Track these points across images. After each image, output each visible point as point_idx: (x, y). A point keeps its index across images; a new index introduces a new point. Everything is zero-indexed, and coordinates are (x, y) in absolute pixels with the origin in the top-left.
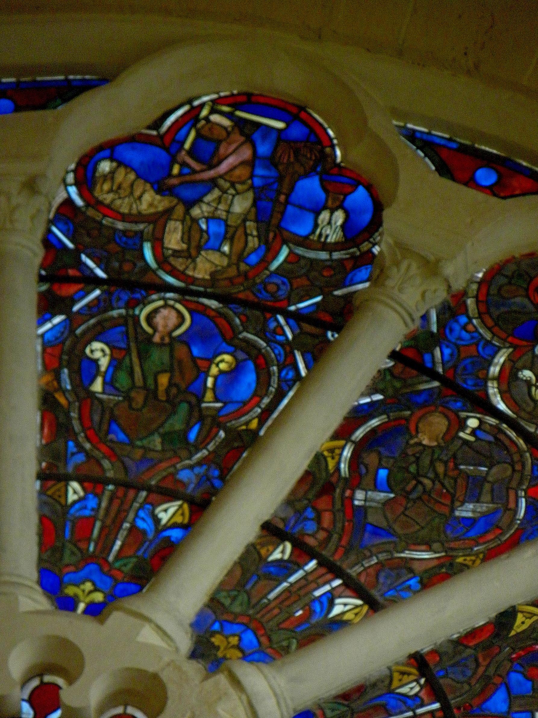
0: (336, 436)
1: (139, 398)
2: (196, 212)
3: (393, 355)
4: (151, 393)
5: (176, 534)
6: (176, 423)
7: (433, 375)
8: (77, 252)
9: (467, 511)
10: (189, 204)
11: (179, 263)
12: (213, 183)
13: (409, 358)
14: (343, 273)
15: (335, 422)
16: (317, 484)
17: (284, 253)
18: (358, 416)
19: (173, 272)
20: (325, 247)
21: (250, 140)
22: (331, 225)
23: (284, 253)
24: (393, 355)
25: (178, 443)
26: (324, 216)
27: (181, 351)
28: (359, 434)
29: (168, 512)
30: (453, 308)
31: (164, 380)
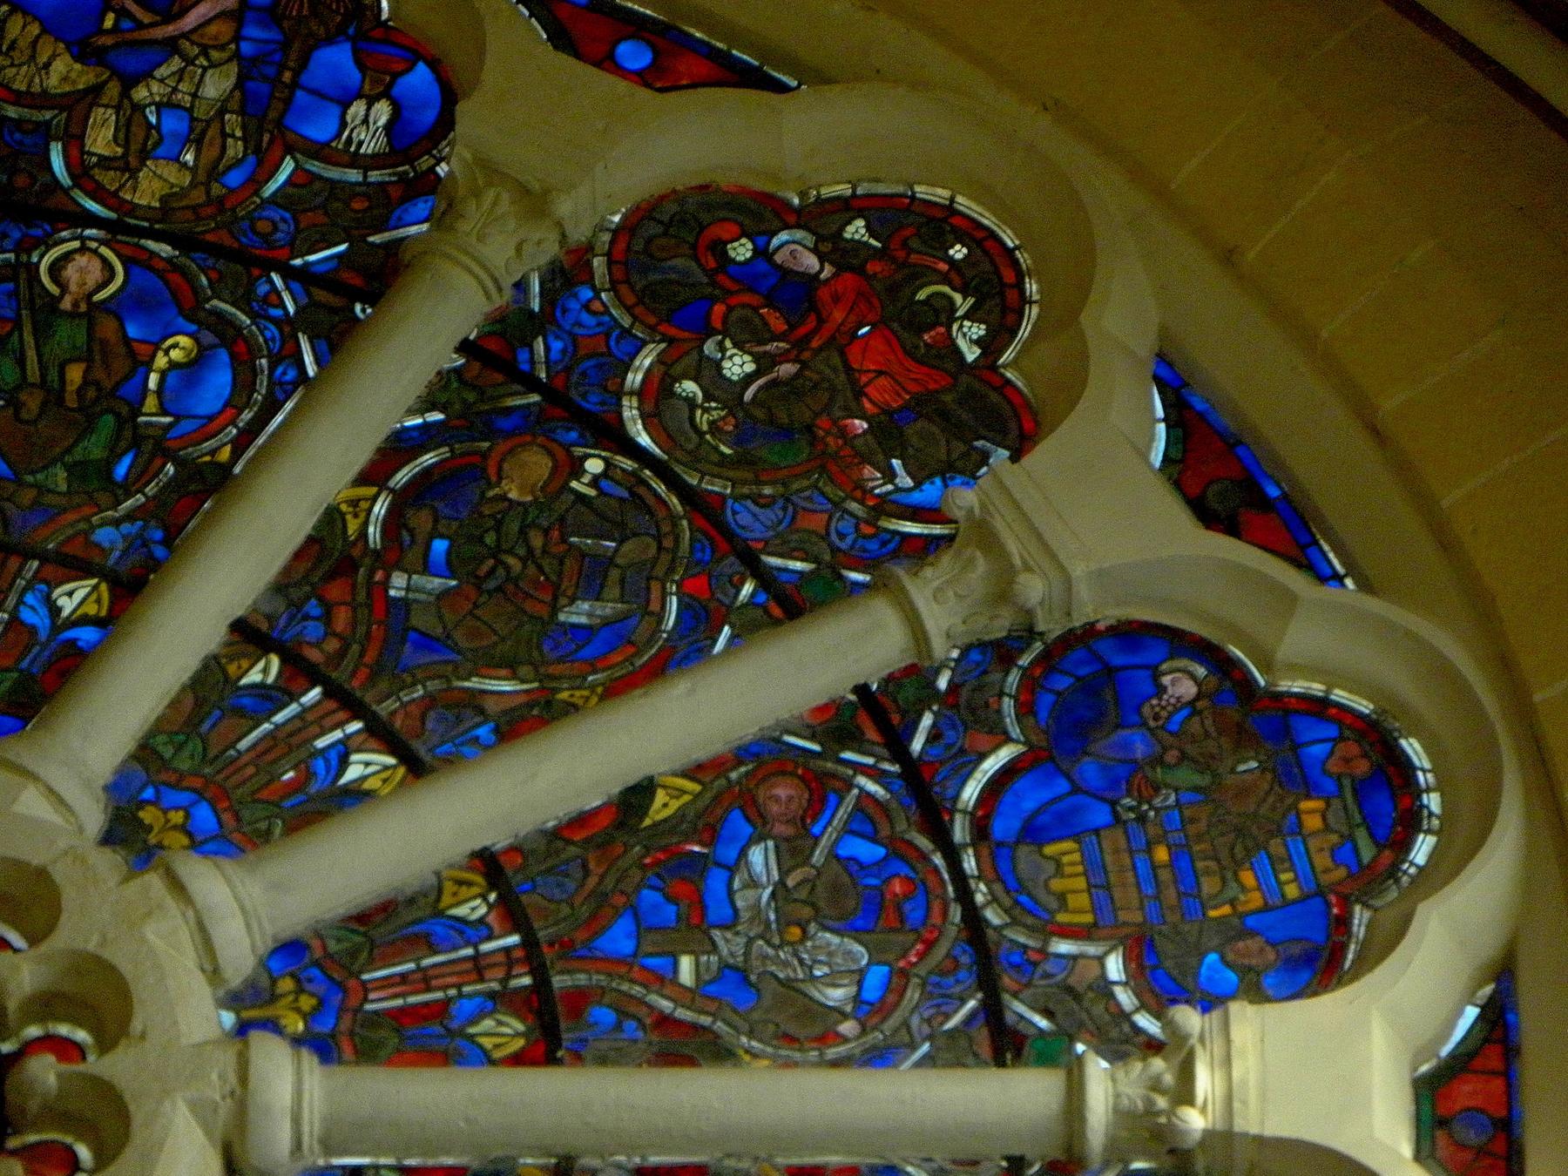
0: (363, 479)
1: (32, 403)
2: (140, 93)
3: (464, 347)
4: (54, 397)
5: (87, 635)
6: (94, 448)
7: (532, 384)
9: (578, 613)
10: (129, 81)
11: (108, 179)
12: (171, 46)
13: (491, 353)
14: (385, 206)
15: (361, 455)
16: (326, 557)
17: (288, 167)
18: (399, 447)
19: (98, 194)
20: (356, 161)
22: (369, 124)
23: (288, 167)
24: (464, 347)
25: (95, 481)
26: (357, 109)
27: (107, 327)
28: (402, 477)
29: (73, 597)
30: (567, 274)
31: (75, 374)
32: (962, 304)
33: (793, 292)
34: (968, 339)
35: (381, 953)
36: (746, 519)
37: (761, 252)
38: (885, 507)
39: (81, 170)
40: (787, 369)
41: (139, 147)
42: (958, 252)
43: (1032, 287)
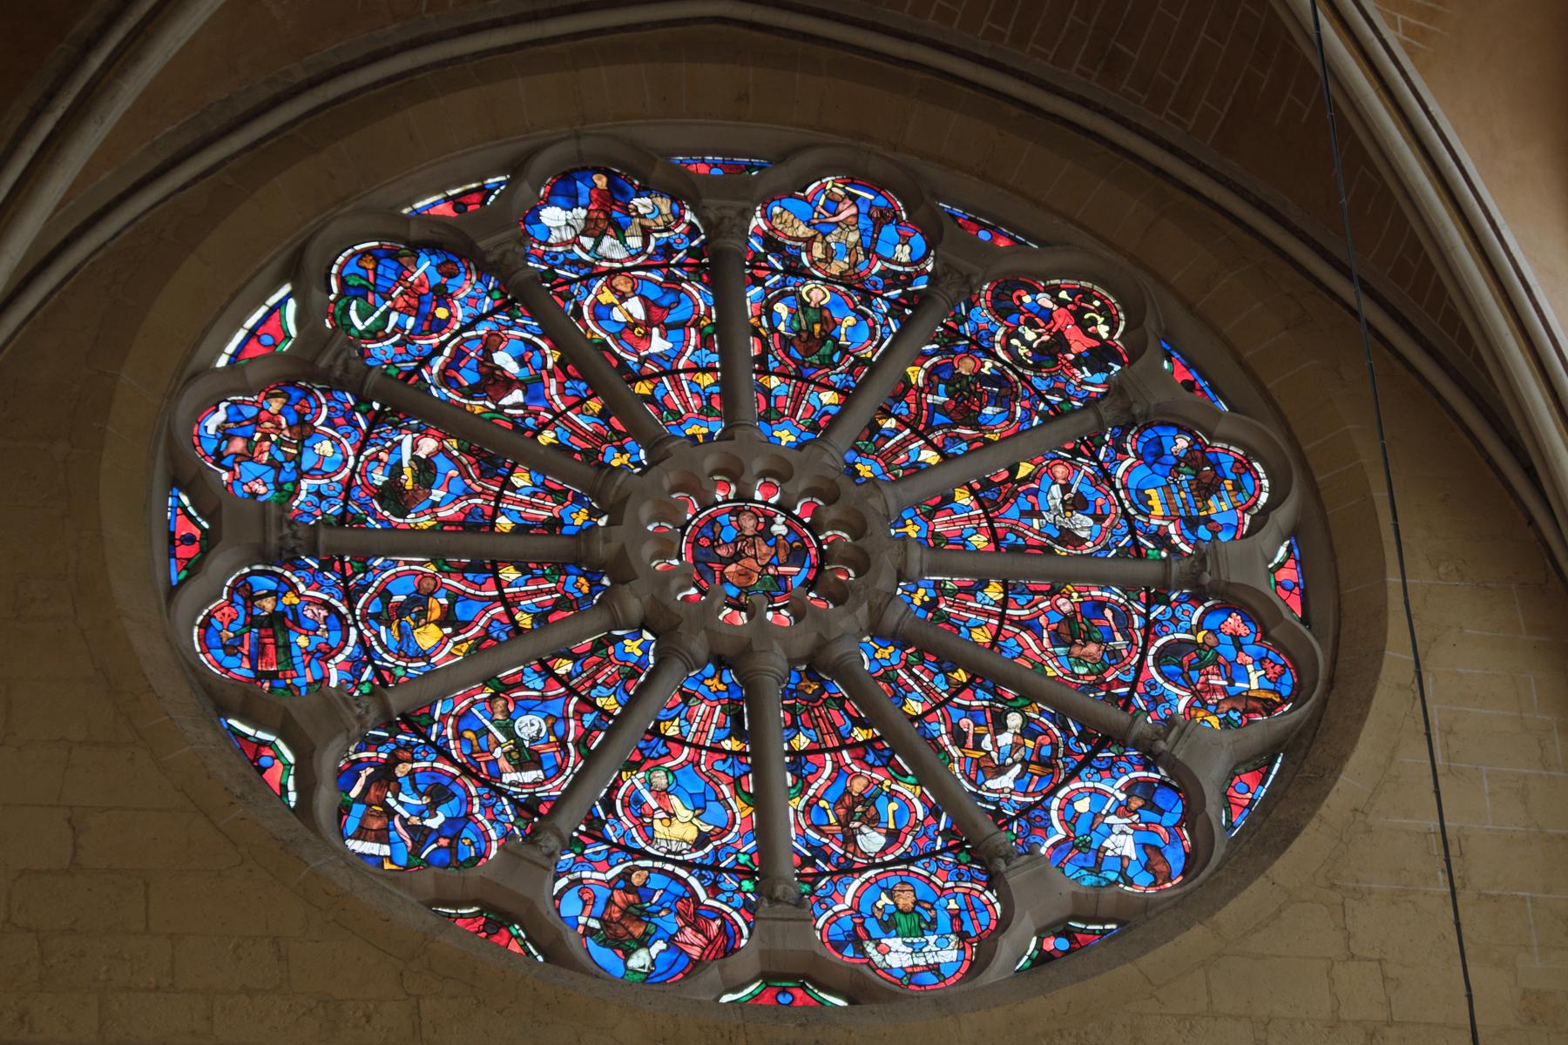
1: (804, 335)
2: (828, 239)
4: (811, 333)
6: (825, 350)
7: (965, 337)
8: (765, 255)
12: (837, 224)
14: (910, 278)
20: (900, 264)
21: (854, 203)
28: (927, 365)
29: (829, 397)
31: (817, 327)
32: (1100, 320)
33: (1048, 315)
34: (1103, 330)
36: (1037, 382)
37: (1034, 300)
38: (1083, 382)
39: (813, 263)
40: (1046, 338)
41: (829, 256)
42: (1097, 303)
43: (1122, 315)
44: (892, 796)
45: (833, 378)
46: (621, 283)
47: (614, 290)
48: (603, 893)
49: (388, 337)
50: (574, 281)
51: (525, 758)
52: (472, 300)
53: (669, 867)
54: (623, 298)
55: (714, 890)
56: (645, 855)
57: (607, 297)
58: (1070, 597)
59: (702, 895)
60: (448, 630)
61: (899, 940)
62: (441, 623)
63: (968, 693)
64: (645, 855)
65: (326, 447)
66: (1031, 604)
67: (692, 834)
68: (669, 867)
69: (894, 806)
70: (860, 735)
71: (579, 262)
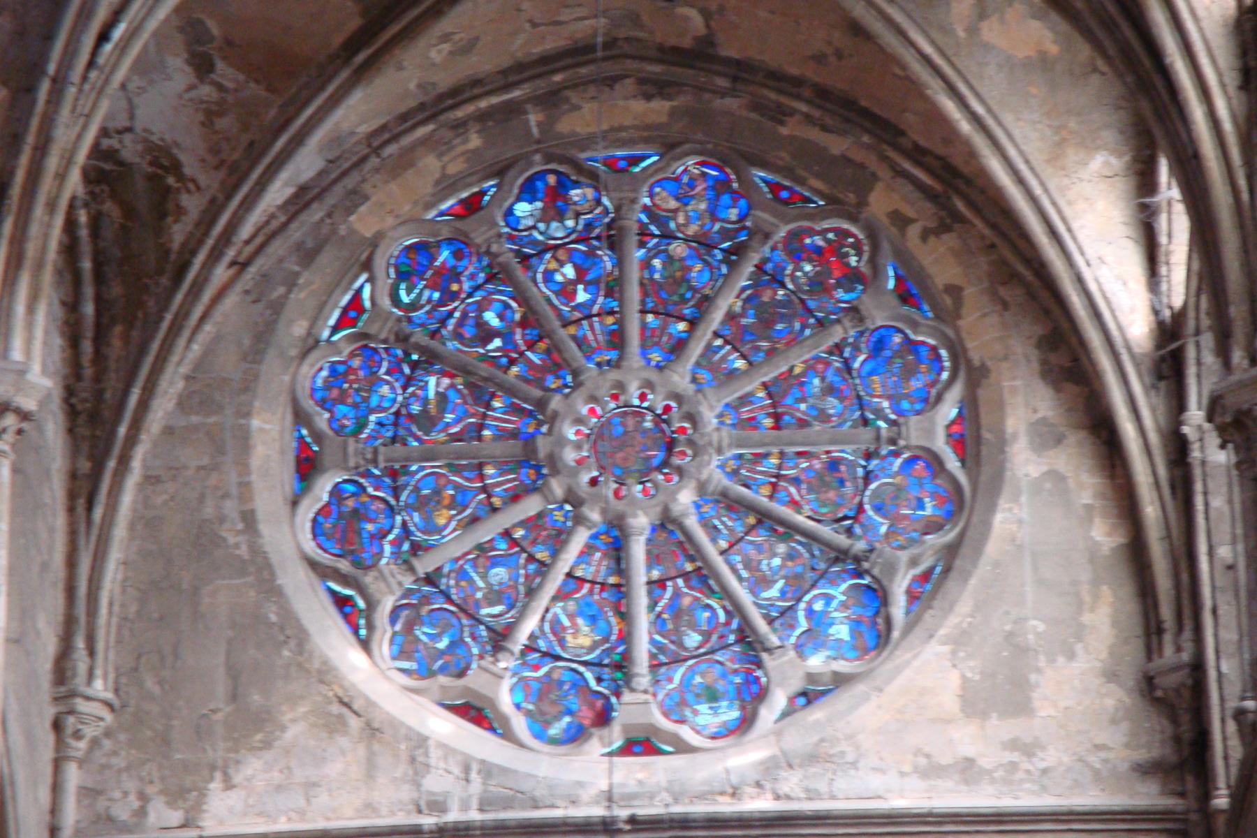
35: (744, 405)
44: (708, 607)
45: (687, 312)
46: (561, 254)
47: (557, 260)
48: (535, 685)
49: (422, 306)
50: (533, 255)
51: (495, 596)
52: (472, 277)
53: (574, 666)
54: (562, 264)
55: (599, 680)
56: (558, 658)
57: (553, 265)
58: (819, 458)
59: (593, 683)
60: (453, 512)
61: (706, 706)
62: (450, 507)
63: (754, 532)
64: (558, 658)
65: (385, 389)
66: (796, 466)
67: (586, 641)
68: (574, 666)
69: (707, 614)
70: (689, 567)
71: (535, 243)
